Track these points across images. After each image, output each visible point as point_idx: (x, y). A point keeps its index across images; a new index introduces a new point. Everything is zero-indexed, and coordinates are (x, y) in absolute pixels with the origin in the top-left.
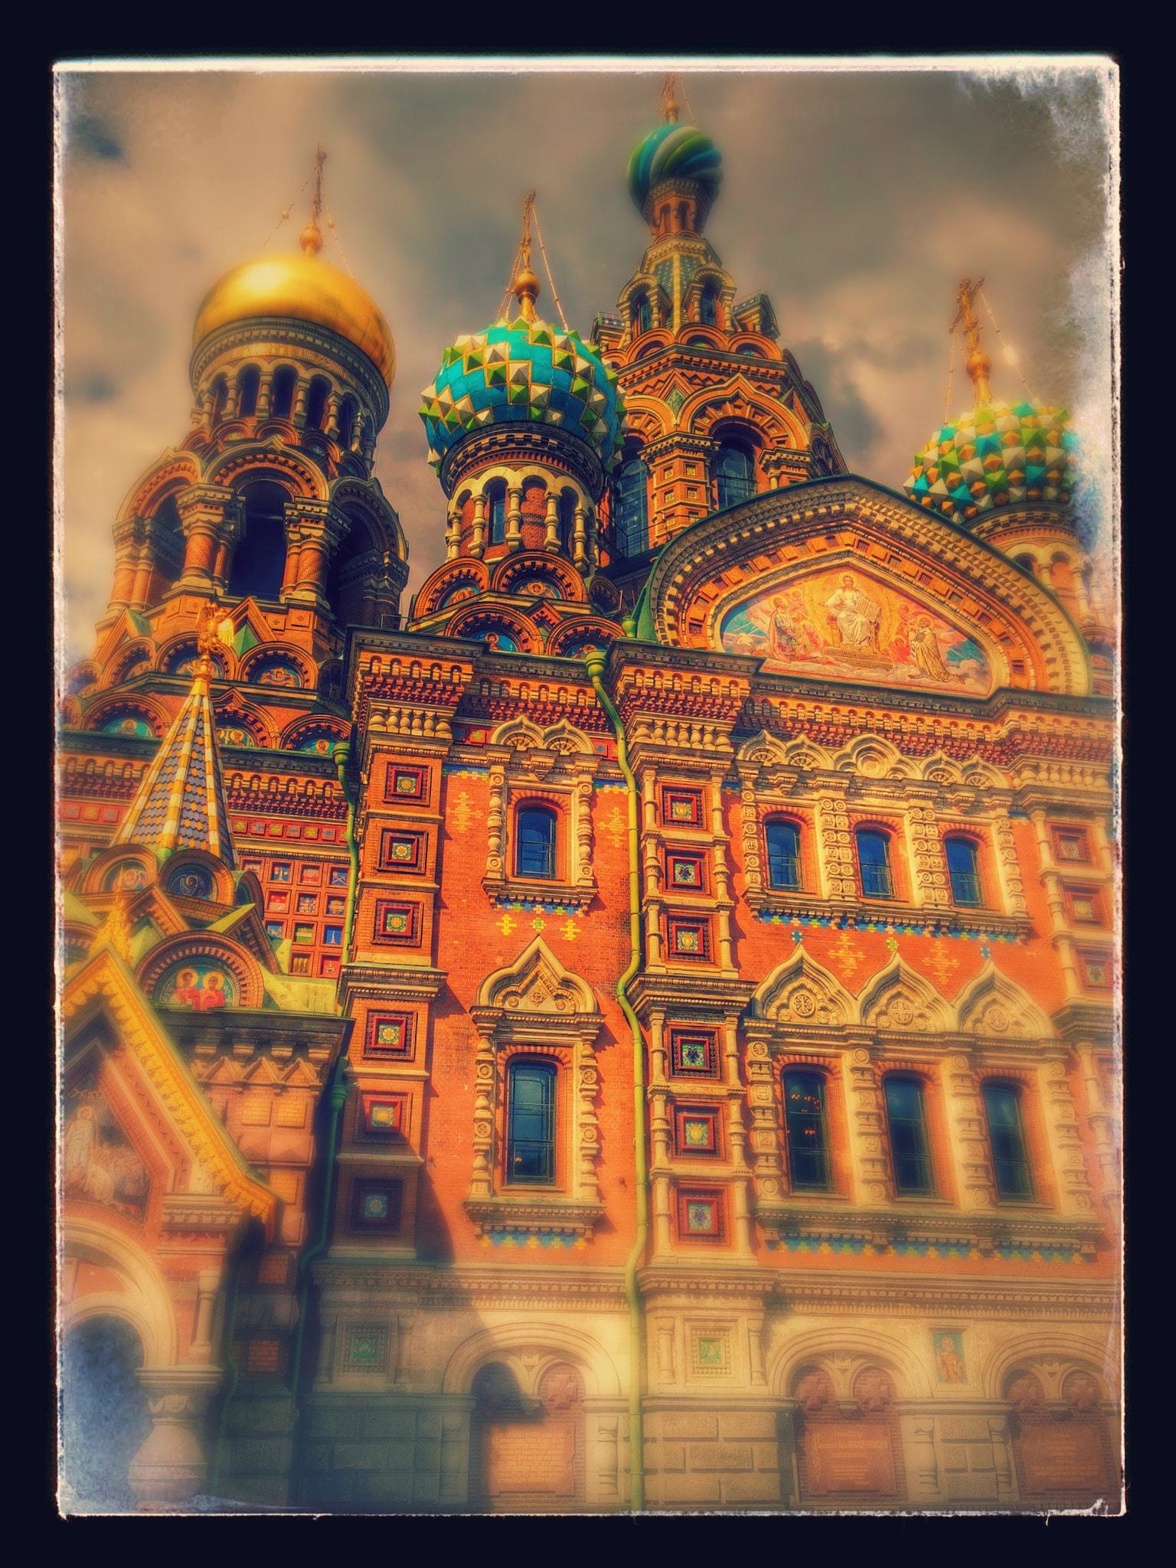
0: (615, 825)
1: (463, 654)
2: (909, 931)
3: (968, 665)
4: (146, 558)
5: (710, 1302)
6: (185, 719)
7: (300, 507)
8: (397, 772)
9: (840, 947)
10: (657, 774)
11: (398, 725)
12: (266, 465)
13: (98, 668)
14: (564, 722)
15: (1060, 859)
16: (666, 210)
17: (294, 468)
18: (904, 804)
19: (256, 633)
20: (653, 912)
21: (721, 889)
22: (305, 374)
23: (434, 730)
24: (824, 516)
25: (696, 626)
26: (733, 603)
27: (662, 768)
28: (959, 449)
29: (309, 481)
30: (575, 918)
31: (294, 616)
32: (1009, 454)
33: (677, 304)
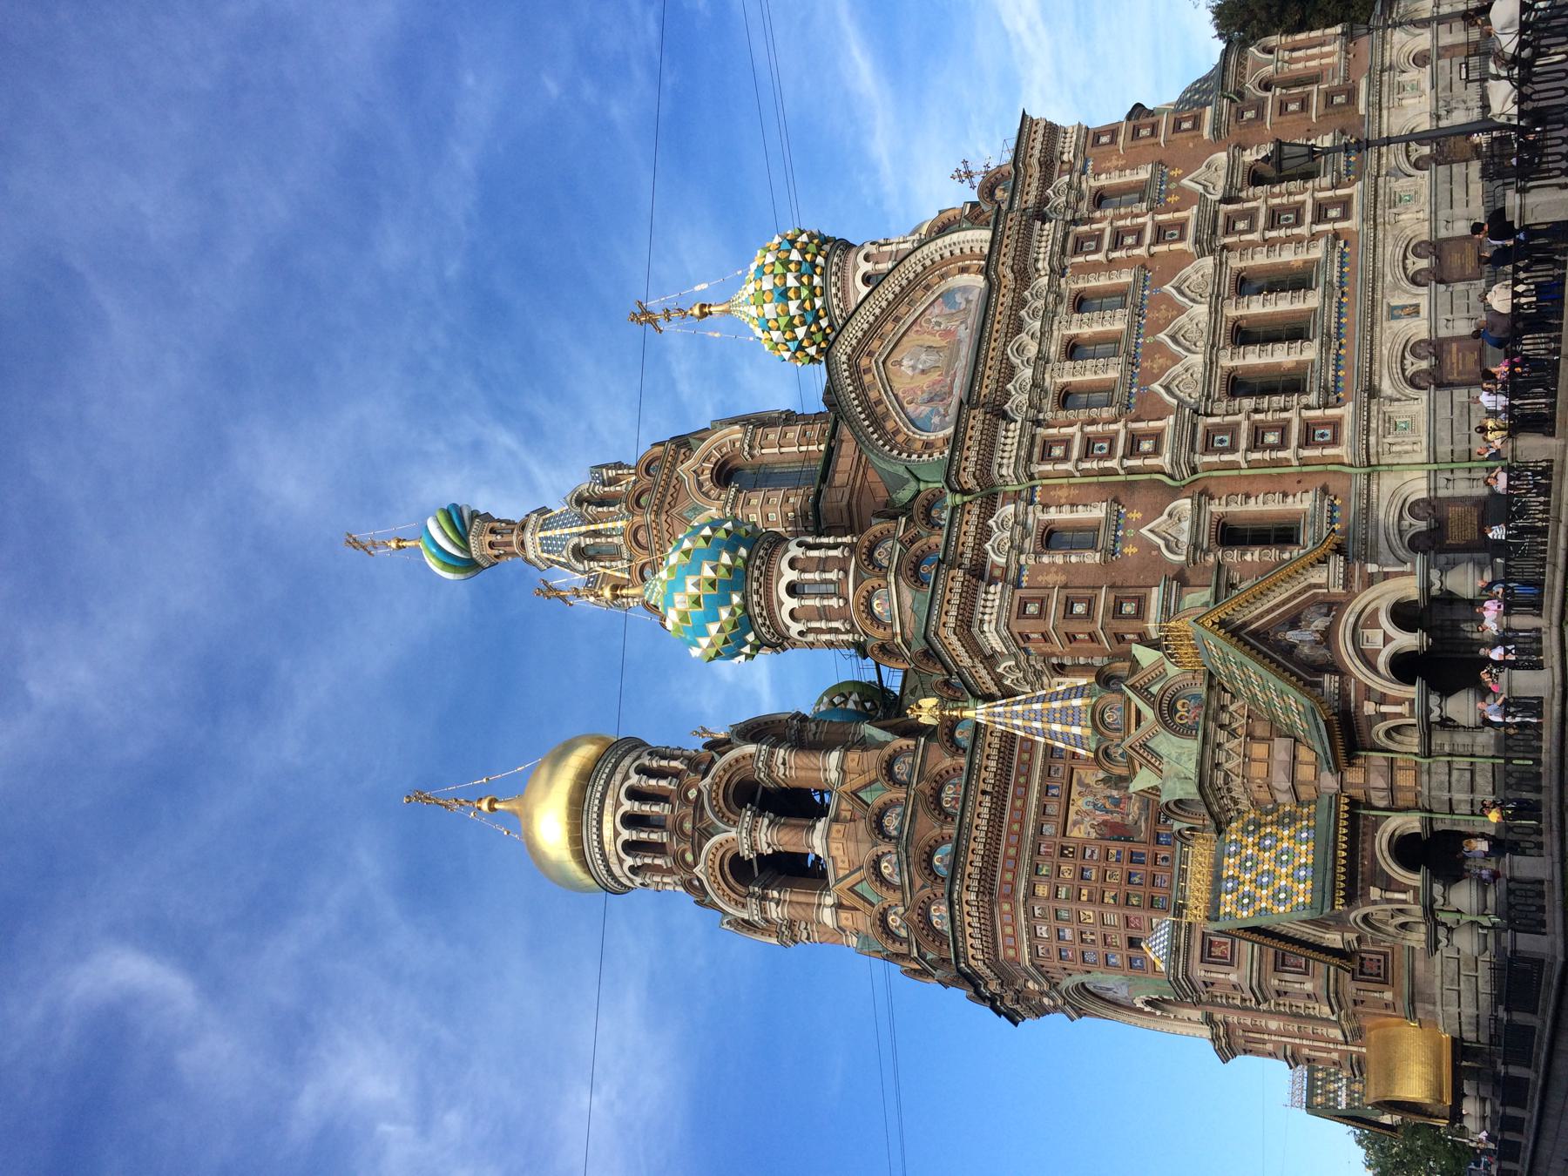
0: (1063, 493)
2: (1141, 331)
3: (959, 298)
4: (779, 893)
5: (1373, 425)
6: (994, 715)
7: (760, 764)
9: (1152, 368)
12: (721, 792)
13: (878, 908)
14: (991, 522)
15: (1097, 250)
16: (492, 545)
17: (724, 770)
18: (1055, 333)
19: (865, 786)
20: (1129, 463)
21: (1113, 427)
22: (634, 779)
25: (928, 445)
28: (778, 315)
30: (1128, 512)
32: (791, 281)
33: (592, 527)
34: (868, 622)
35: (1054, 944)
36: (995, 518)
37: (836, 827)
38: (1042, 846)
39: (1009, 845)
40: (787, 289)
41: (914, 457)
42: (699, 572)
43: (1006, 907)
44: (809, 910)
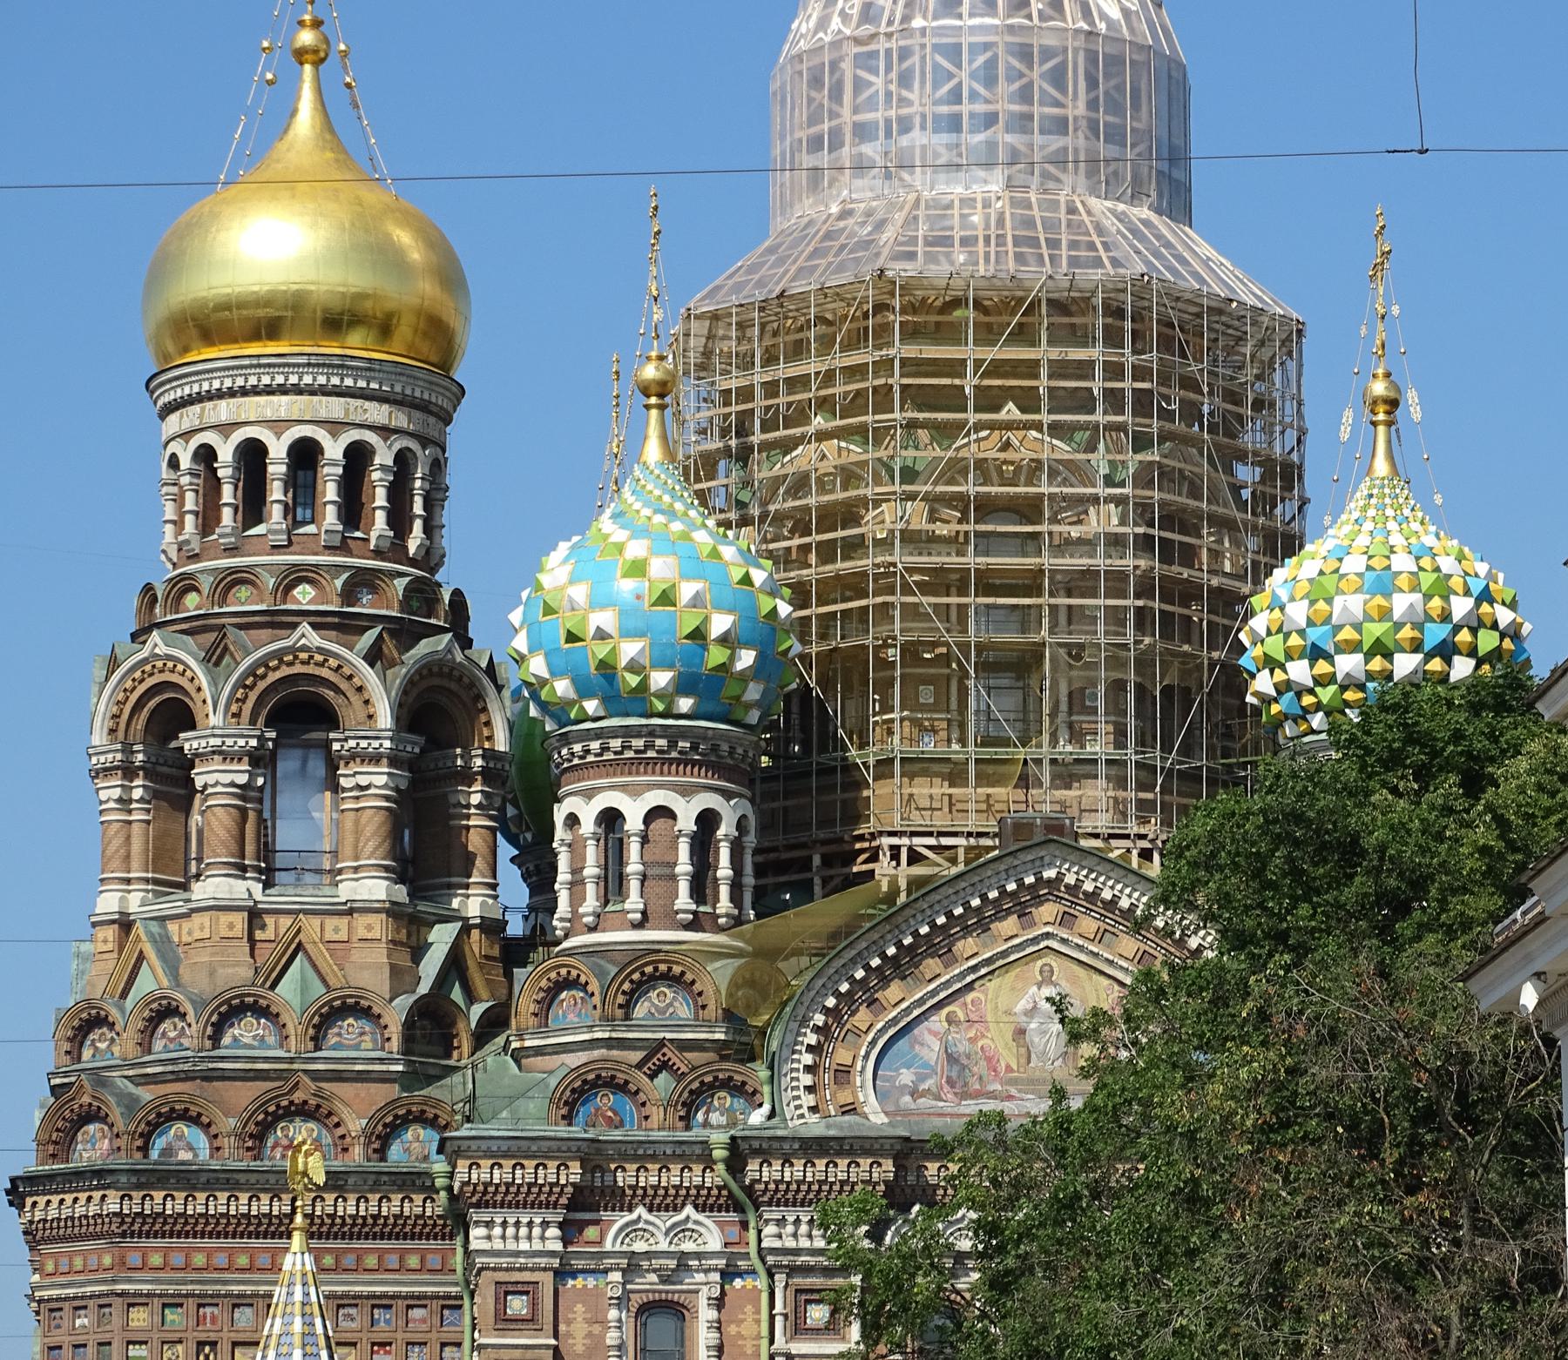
1: (569, 1150)
7: (352, 743)
8: (506, 1290)
10: (788, 1276)
11: (503, 1237)
12: (298, 669)
13: (114, 1014)
14: (689, 1210)
19: (314, 966)
22: (334, 449)
23: (543, 1238)
24: (1013, 894)
25: (843, 1074)
26: (891, 1032)
27: (793, 1271)
29: (360, 689)
31: (361, 921)
32: (1348, 664)
34: (544, 983)
35: (67, 1339)
36: (695, 1215)
37: (239, 920)
38: (216, 1310)
39: (210, 1253)
40: (1329, 658)
41: (808, 1059)
42: (627, 634)
43: (107, 1261)
44: (115, 863)
